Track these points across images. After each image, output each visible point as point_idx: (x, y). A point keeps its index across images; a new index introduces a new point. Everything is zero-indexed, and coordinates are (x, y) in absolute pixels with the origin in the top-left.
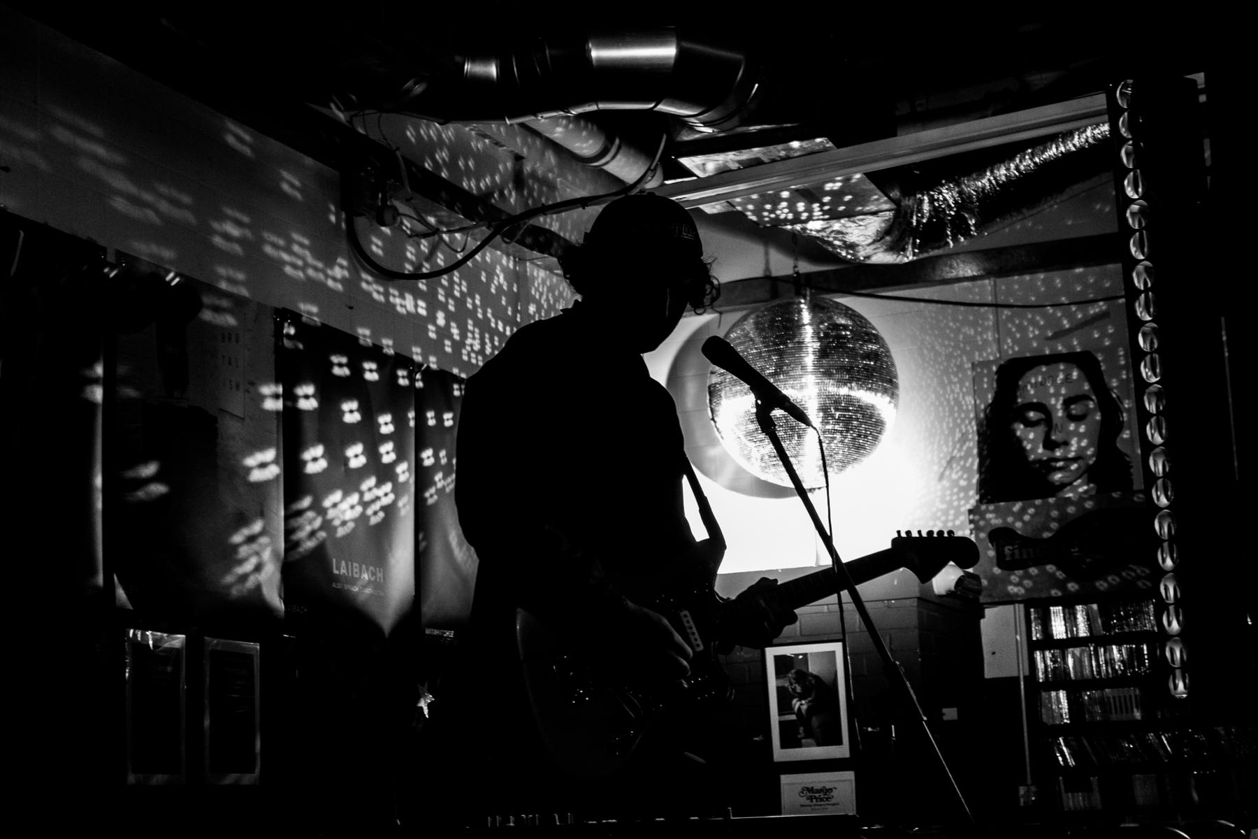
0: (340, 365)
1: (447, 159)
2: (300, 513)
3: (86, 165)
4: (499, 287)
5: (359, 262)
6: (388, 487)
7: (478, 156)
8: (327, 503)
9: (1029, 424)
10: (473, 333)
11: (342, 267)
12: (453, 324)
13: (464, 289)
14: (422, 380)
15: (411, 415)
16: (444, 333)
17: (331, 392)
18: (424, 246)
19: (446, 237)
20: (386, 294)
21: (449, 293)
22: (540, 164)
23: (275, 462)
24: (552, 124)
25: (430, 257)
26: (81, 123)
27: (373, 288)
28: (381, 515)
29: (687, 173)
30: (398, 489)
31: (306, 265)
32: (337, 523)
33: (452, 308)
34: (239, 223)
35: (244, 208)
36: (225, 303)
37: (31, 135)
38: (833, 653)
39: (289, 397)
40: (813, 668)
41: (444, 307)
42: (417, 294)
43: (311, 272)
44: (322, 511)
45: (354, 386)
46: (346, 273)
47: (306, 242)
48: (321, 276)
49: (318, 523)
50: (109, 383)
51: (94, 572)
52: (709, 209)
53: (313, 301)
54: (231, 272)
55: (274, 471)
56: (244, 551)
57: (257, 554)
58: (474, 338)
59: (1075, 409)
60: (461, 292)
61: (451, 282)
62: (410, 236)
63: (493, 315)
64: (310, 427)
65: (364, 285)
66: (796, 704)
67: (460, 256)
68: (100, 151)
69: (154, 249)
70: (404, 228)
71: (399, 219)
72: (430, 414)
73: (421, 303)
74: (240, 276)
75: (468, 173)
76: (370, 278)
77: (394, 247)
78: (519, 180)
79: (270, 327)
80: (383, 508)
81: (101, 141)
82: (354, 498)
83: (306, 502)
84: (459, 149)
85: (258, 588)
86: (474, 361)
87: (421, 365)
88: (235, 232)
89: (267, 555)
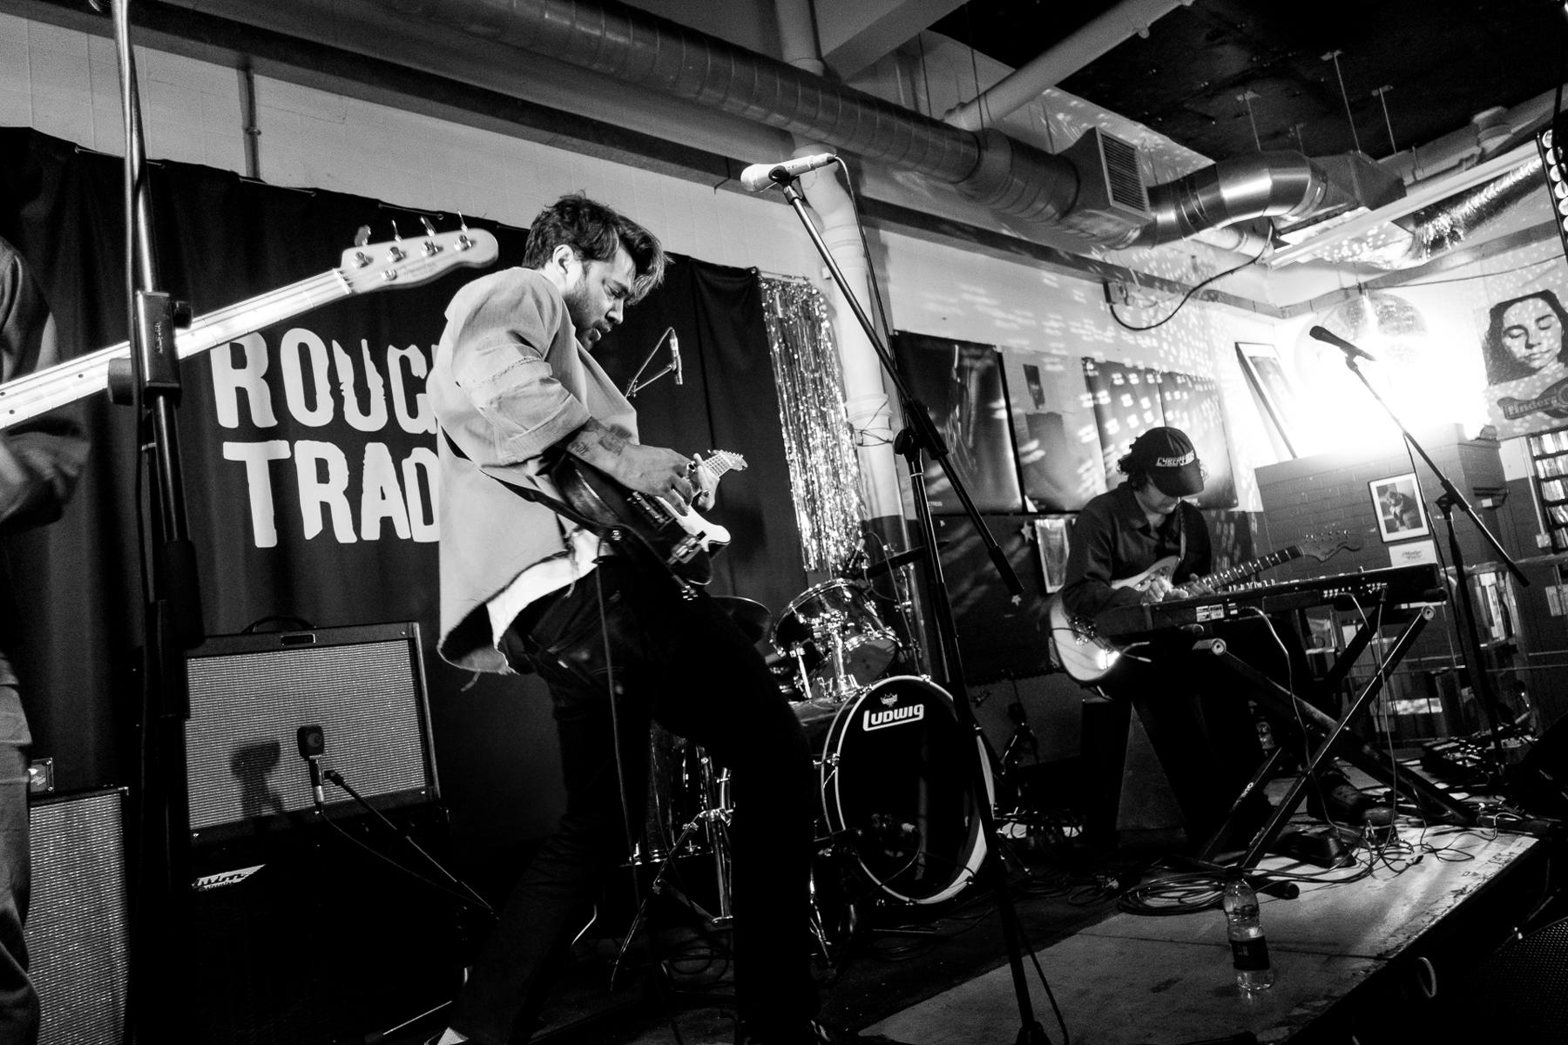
2: (1109, 454)
3: (980, 309)
4: (1194, 324)
9: (1513, 337)
16: (1168, 353)
17: (1115, 391)
18: (1151, 311)
20: (1136, 340)
22: (1205, 257)
24: (1207, 235)
26: (973, 289)
27: (1127, 336)
29: (1285, 244)
33: (1170, 339)
34: (1058, 321)
36: (1057, 360)
37: (952, 300)
38: (1410, 481)
39: (1094, 398)
40: (1400, 490)
41: (1166, 340)
42: (1151, 336)
43: (1096, 337)
45: (1126, 387)
46: (1114, 334)
47: (1091, 322)
48: (1101, 338)
50: (1008, 407)
51: (1014, 497)
52: (1302, 260)
56: (1085, 476)
59: (1543, 324)
61: (1168, 327)
64: (1107, 412)
66: (1392, 509)
68: (986, 300)
73: (1154, 341)
74: (1062, 345)
78: (1195, 268)
79: (1081, 367)
86: (1186, 364)
88: (1056, 325)
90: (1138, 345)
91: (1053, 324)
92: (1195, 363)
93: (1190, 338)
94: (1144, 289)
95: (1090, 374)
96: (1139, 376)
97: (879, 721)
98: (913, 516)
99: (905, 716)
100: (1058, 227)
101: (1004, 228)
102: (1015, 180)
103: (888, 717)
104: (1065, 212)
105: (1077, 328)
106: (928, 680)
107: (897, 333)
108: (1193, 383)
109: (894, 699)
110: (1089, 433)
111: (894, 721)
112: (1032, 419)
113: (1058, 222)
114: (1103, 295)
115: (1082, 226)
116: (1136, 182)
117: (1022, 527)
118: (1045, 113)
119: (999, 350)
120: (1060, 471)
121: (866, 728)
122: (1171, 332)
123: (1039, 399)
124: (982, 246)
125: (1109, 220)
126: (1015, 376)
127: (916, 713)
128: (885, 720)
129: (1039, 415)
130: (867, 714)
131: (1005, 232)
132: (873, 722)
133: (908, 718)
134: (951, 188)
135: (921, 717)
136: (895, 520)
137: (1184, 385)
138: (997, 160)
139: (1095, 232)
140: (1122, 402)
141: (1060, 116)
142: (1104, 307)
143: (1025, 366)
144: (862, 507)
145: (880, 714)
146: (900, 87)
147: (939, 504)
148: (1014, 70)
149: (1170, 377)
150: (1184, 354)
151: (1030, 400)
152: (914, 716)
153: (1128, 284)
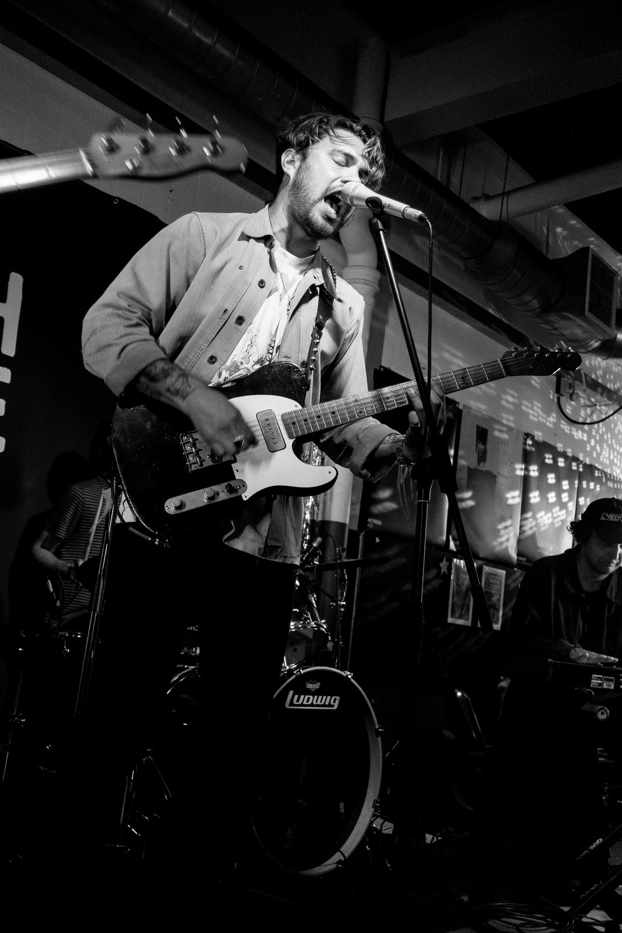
0: (549, 458)
1: (602, 375)
2: (526, 519)
5: (562, 417)
6: (564, 512)
7: (615, 374)
8: (538, 516)
10: (606, 449)
11: (553, 417)
12: (598, 445)
13: (604, 430)
14: (583, 467)
15: (576, 482)
16: (593, 448)
17: (544, 469)
18: (589, 410)
19: (598, 407)
20: (571, 430)
21: (597, 432)
23: (519, 496)
25: (591, 416)
26: (454, 351)
27: (565, 427)
28: (560, 523)
30: (568, 513)
31: (539, 415)
32: (541, 524)
33: (598, 438)
34: (513, 396)
35: (517, 391)
36: (504, 429)
39: (527, 469)
41: (595, 438)
42: (584, 431)
43: (540, 419)
44: (535, 519)
45: (554, 468)
46: (555, 420)
47: (540, 406)
48: (545, 421)
49: (534, 524)
51: (441, 534)
53: (541, 431)
54: (508, 416)
55: (518, 500)
56: (502, 532)
57: (508, 534)
58: (606, 451)
60: (603, 432)
61: (599, 427)
62: (583, 406)
63: (615, 442)
64: (533, 484)
65: (562, 426)
67: (603, 417)
69: (478, 405)
70: (581, 402)
71: (579, 399)
72: (584, 483)
73: (585, 435)
74: (511, 418)
75: (610, 381)
76: (564, 423)
77: (576, 410)
79: (522, 440)
80: (562, 521)
81: (462, 359)
82: (550, 515)
83: (529, 515)
84: (608, 370)
85: (507, 548)
86: (605, 462)
87: (582, 462)
88: (510, 399)
89: (512, 535)
90: (572, 436)
91: (509, 399)
92: (612, 462)
93: (614, 442)
94: (589, 391)
95: (528, 448)
96: (565, 462)
97: (300, 702)
98: (355, 528)
99: (323, 703)
100: (536, 320)
101: (491, 307)
102: (515, 271)
103: (308, 701)
104: (547, 309)
105: (526, 406)
106: (350, 677)
107: (382, 369)
108: (607, 479)
109: (317, 686)
110: (514, 497)
111: (312, 705)
112: (472, 473)
113: (539, 315)
114: (555, 386)
115: (557, 325)
116: (610, 302)
117: (442, 561)
118: (548, 223)
119: (461, 407)
120: (484, 523)
121: (287, 705)
122: (601, 432)
123: (482, 457)
124: (470, 317)
125: (580, 326)
126: (468, 433)
127: (332, 703)
128: (305, 703)
129: (478, 470)
130: (291, 693)
131: (491, 311)
132: (295, 702)
133: (324, 705)
134: (460, 264)
135: (335, 707)
136: (343, 525)
137: (600, 478)
138: (504, 250)
139: (565, 333)
140: (547, 479)
141: (559, 230)
142: (552, 396)
143: (478, 427)
144: (316, 508)
145: (302, 697)
146: (440, 166)
147: (379, 523)
148: (534, 181)
149: (590, 469)
150: (605, 453)
151: (475, 457)
152: (330, 705)
153: (577, 383)
